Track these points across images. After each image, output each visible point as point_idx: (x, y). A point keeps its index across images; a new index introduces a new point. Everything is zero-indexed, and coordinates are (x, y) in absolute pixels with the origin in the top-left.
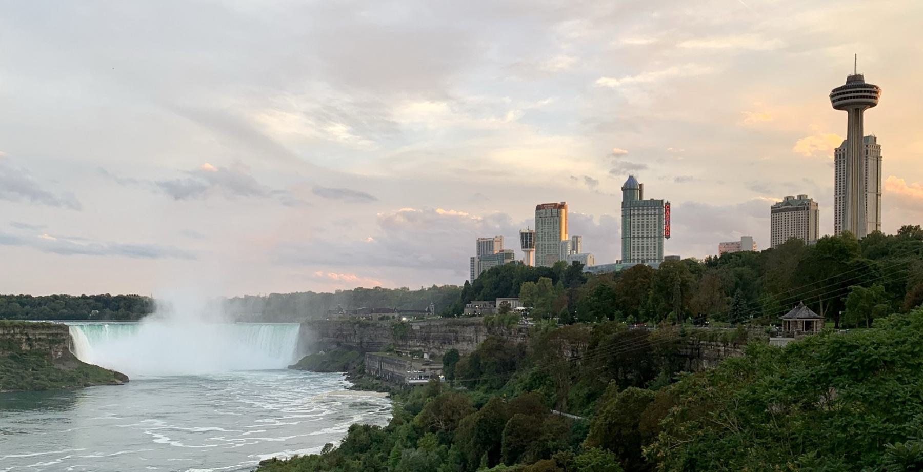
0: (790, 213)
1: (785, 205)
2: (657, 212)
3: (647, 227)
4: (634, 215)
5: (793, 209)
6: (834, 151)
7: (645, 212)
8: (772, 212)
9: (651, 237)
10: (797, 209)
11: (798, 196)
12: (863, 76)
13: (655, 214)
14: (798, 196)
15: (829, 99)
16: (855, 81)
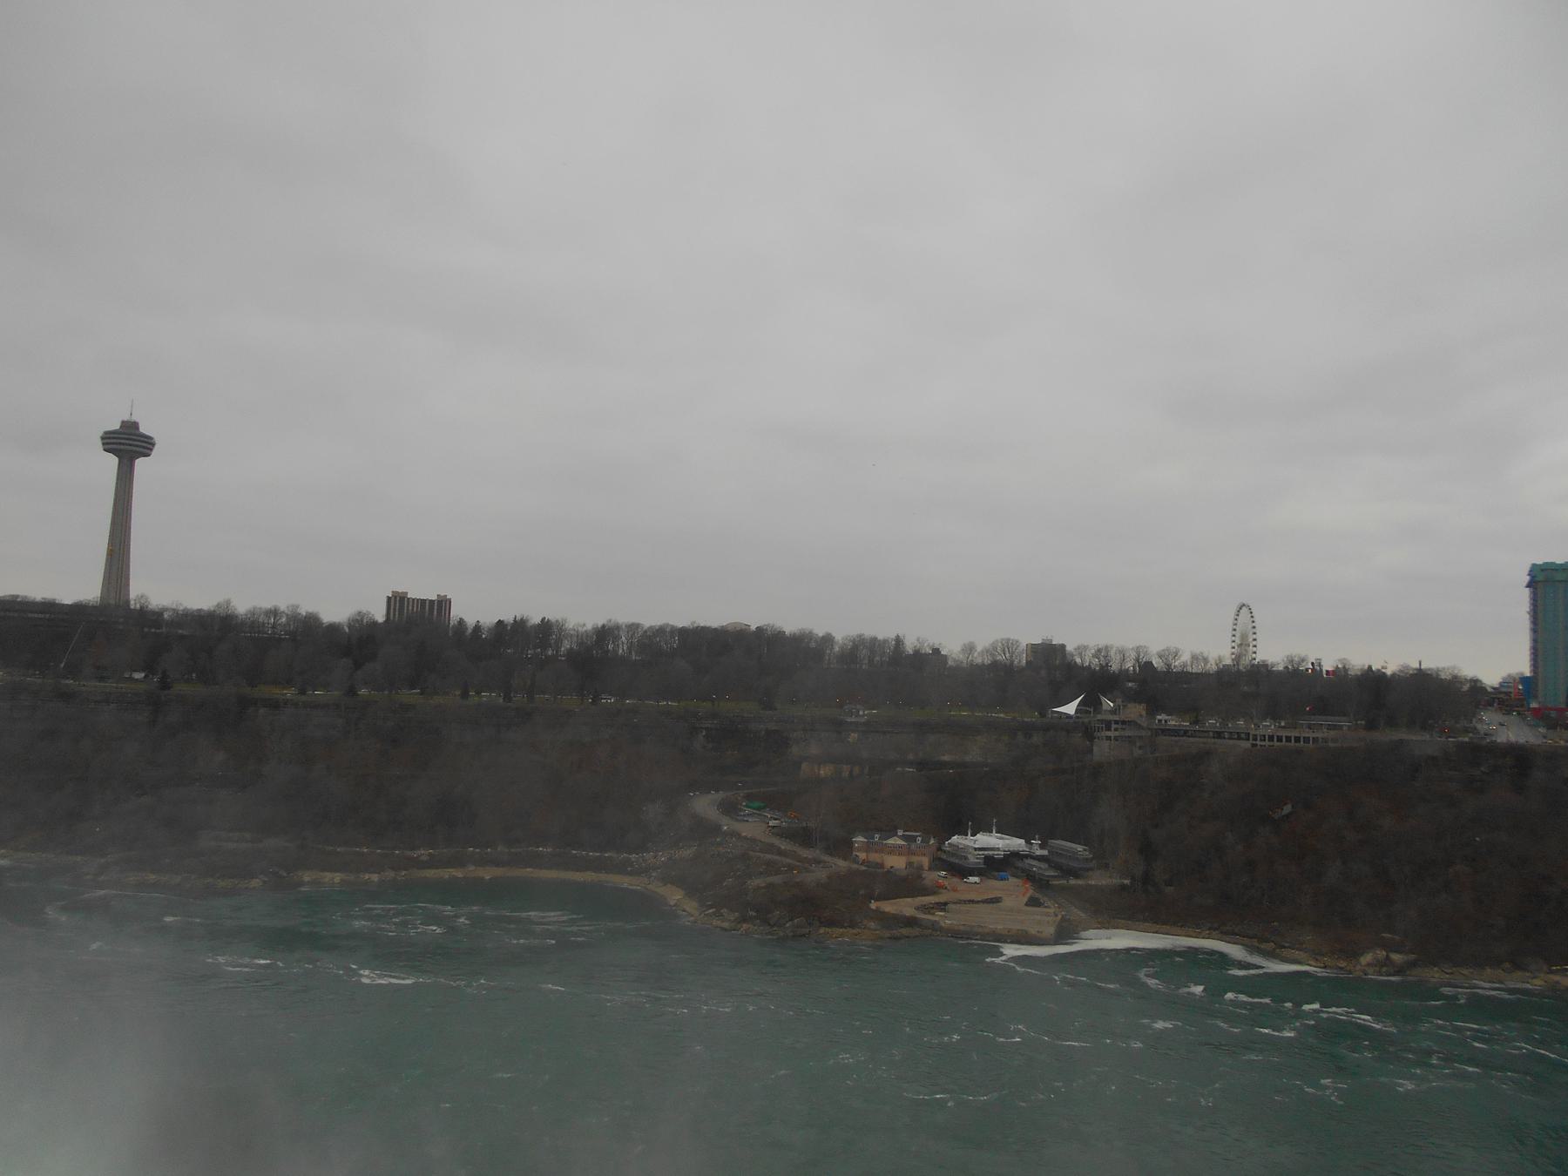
12: (138, 424)
15: (100, 439)
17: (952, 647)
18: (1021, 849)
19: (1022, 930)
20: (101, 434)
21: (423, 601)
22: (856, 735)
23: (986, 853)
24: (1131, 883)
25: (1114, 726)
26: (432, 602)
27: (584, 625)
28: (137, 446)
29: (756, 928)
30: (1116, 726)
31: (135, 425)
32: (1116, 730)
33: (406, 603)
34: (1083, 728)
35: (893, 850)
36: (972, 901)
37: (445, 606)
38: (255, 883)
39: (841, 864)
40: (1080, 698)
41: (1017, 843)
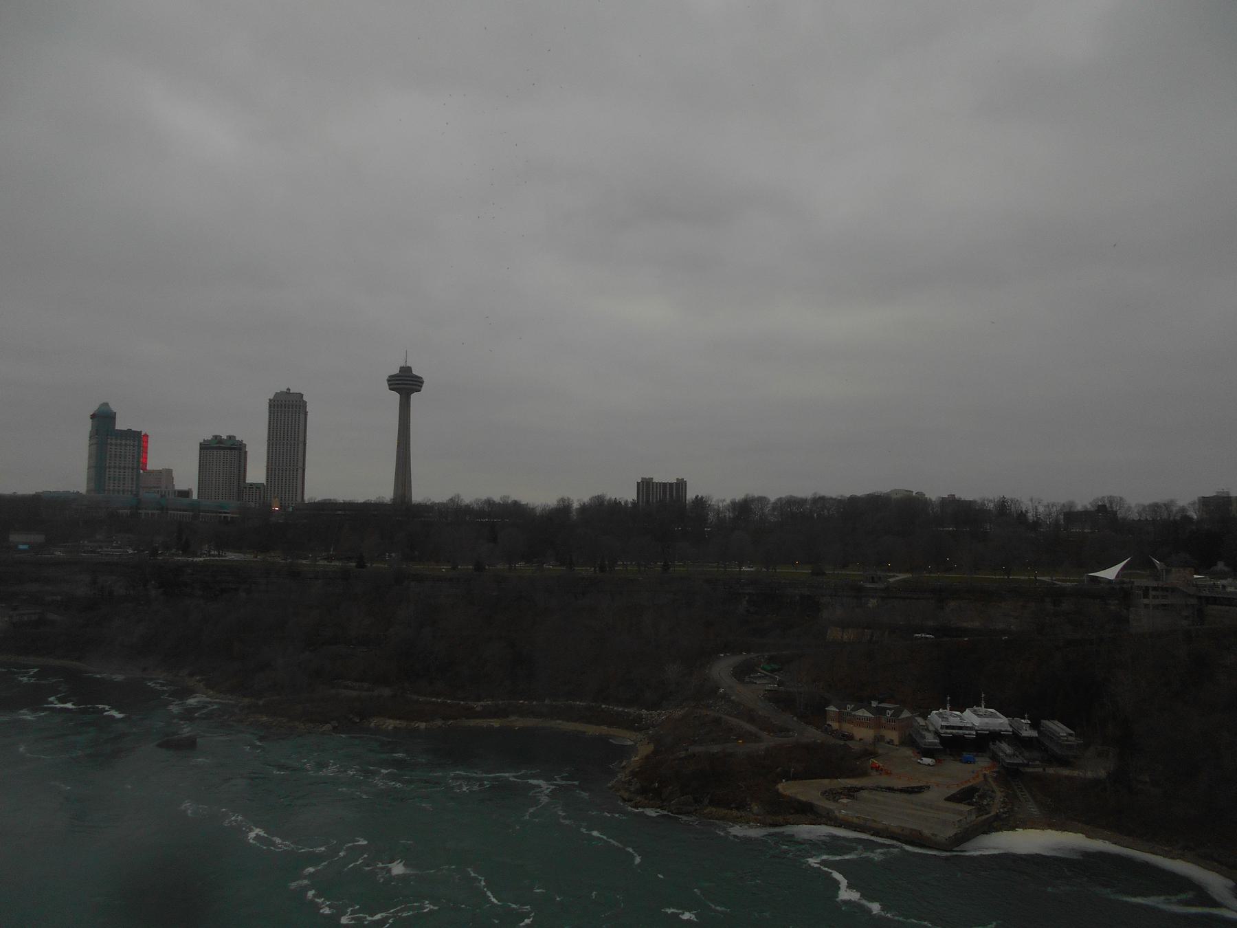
0: (222, 452)
1: (217, 444)
2: (136, 443)
3: (125, 458)
4: (111, 444)
5: (224, 448)
6: (268, 401)
7: (123, 442)
8: (201, 449)
9: (129, 468)
10: (230, 449)
11: (227, 436)
13: (134, 446)
14: (227, 436)
15: (386, 382)
16: (406, 370)
17: (1026, 505)
18: (1003, 729)
19: (915, 830)
20: (387, 377)
21: (665, 484)
22: (875, 601)
23: (954, 731)
24: (316, 891)
25: (1152, 593)
26: (671, 484)
27: (724, 500)
28: (410, 384)
29: (646, 802)
30: (1154, 593)
31: (409, 369)
32: (1154, 597)
33: (651, 486)
34: (1118, 590)
35: (862, 722)
36: (891, 789)
37: (682, 488)
38: (328, 727)
39: (812, 734)
40: (1125, 562)
41: (1000, 722)
